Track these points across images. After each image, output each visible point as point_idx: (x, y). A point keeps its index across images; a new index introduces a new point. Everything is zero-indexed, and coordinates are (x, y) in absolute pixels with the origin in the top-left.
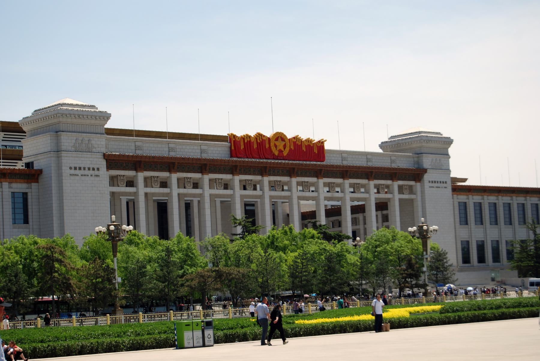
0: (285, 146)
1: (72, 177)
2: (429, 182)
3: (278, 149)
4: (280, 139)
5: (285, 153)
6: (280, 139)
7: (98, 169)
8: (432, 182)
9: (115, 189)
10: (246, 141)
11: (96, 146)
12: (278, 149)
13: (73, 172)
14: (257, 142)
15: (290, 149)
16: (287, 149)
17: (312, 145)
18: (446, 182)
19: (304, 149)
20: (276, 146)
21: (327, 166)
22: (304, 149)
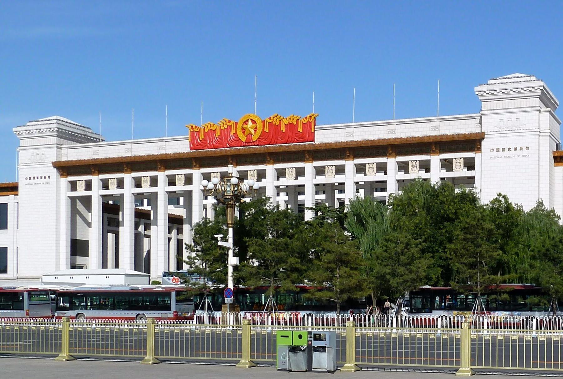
0: (256, 129)
1: (28, 186)
2: (26, 179)
3: (246, 133)
4: (250, 123)
5: (255, 138)
6: (250, 123)
7: (49, 177)
8: (498, 150)
9: (172, 189)
10: (206, 131)
11: (48, 156)
12: (246, 133)
13: (28, 181)
14: (221, 130)
15: (263, 131)
16: (259, 132)
17: (295, 123)
18: (528, 148)
19: (283, 129)
20: (244, 130)
21: (320, 144)
22: (283, 129)
